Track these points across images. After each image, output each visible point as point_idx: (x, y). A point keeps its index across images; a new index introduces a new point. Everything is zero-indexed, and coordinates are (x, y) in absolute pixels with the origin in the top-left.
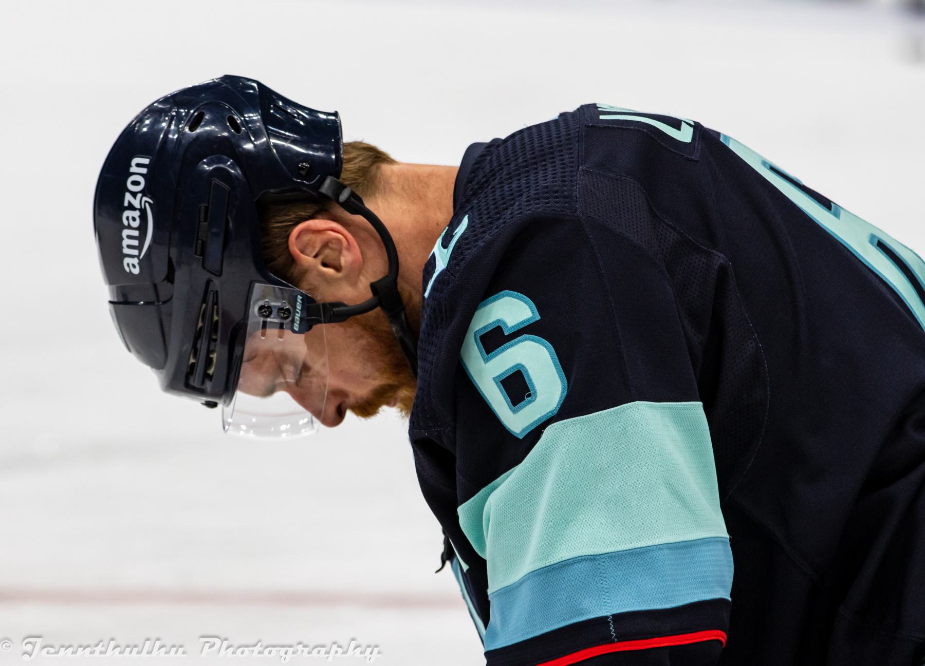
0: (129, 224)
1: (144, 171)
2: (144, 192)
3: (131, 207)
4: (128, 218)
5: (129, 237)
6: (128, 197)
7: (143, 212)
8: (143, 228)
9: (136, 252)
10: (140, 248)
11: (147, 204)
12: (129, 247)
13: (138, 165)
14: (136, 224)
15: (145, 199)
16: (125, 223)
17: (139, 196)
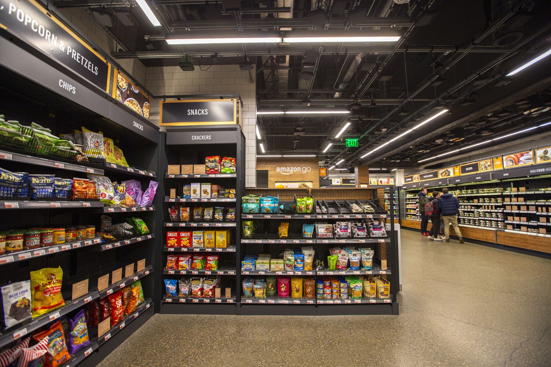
1: (298, 171)
2: (294, 172)
3: (290, 169)
6: (292, 168)
7: (290, 172)
9: (281, 171)
10: (282, 172)
14: (287, 171)
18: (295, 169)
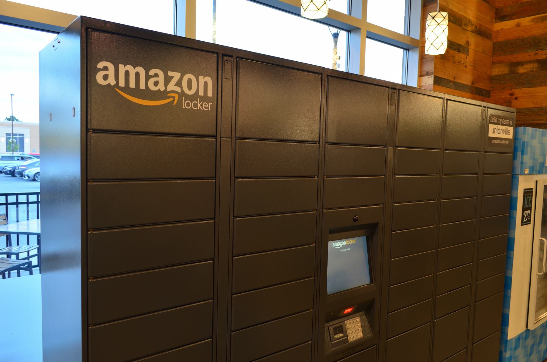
0: (152, 77)
1: (201, 93)
2: (182, 94)
3: (168, 80)
4: (156, 75)
5: (137, 74)
6: (176, 76)
8: (147, 94)
9: (122, 84)
11: (172, 99)
12: (127, 73)
13: (206, 84)
14: (152, 87)
15: (176, 96)
16: (152, 72)
17: (178, 89)
18: (190, 81)
